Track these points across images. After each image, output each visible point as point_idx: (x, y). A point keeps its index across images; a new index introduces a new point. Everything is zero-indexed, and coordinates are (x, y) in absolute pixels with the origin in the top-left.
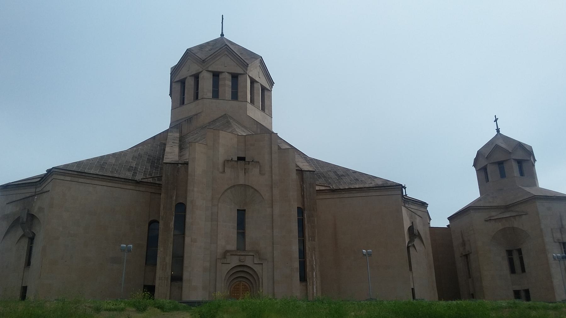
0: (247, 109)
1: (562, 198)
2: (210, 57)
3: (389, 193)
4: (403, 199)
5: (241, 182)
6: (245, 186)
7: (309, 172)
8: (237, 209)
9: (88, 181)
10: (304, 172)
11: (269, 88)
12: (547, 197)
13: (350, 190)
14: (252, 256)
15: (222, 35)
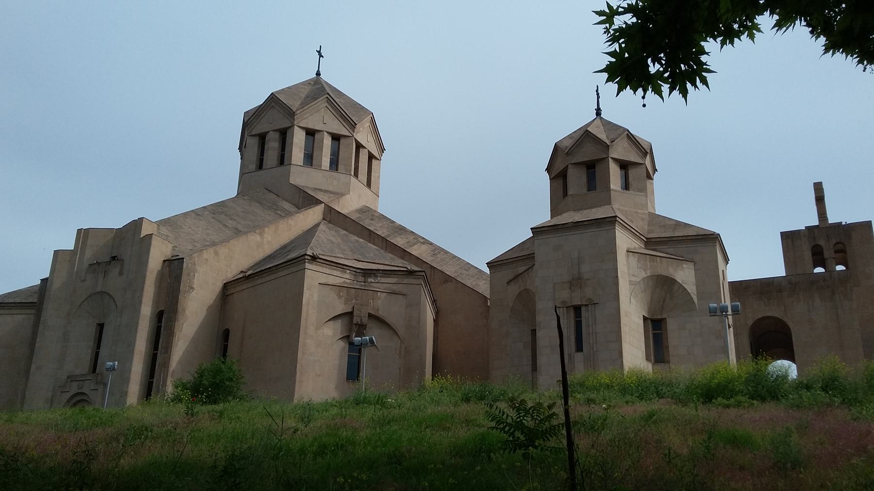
0: (291, 174)
1: (586, 223)
2: (253, 117)
3: (295, 269)
4: (358, 271)
5: (99, 289)
6: (102, 293)
7: (177, 261)
8: (98, 324)
9: (7, 312)
10: (172, 262)
11: (346, 133)
12: (556, 227)
13: (262, 271)
14: (90, 381)
15: (318, 74)
